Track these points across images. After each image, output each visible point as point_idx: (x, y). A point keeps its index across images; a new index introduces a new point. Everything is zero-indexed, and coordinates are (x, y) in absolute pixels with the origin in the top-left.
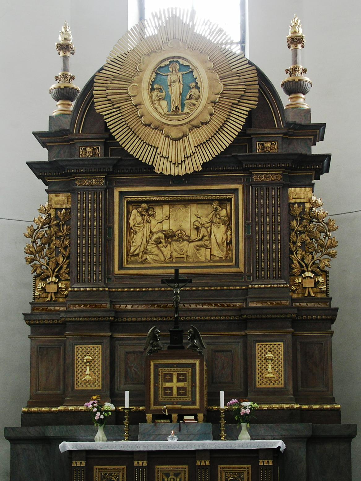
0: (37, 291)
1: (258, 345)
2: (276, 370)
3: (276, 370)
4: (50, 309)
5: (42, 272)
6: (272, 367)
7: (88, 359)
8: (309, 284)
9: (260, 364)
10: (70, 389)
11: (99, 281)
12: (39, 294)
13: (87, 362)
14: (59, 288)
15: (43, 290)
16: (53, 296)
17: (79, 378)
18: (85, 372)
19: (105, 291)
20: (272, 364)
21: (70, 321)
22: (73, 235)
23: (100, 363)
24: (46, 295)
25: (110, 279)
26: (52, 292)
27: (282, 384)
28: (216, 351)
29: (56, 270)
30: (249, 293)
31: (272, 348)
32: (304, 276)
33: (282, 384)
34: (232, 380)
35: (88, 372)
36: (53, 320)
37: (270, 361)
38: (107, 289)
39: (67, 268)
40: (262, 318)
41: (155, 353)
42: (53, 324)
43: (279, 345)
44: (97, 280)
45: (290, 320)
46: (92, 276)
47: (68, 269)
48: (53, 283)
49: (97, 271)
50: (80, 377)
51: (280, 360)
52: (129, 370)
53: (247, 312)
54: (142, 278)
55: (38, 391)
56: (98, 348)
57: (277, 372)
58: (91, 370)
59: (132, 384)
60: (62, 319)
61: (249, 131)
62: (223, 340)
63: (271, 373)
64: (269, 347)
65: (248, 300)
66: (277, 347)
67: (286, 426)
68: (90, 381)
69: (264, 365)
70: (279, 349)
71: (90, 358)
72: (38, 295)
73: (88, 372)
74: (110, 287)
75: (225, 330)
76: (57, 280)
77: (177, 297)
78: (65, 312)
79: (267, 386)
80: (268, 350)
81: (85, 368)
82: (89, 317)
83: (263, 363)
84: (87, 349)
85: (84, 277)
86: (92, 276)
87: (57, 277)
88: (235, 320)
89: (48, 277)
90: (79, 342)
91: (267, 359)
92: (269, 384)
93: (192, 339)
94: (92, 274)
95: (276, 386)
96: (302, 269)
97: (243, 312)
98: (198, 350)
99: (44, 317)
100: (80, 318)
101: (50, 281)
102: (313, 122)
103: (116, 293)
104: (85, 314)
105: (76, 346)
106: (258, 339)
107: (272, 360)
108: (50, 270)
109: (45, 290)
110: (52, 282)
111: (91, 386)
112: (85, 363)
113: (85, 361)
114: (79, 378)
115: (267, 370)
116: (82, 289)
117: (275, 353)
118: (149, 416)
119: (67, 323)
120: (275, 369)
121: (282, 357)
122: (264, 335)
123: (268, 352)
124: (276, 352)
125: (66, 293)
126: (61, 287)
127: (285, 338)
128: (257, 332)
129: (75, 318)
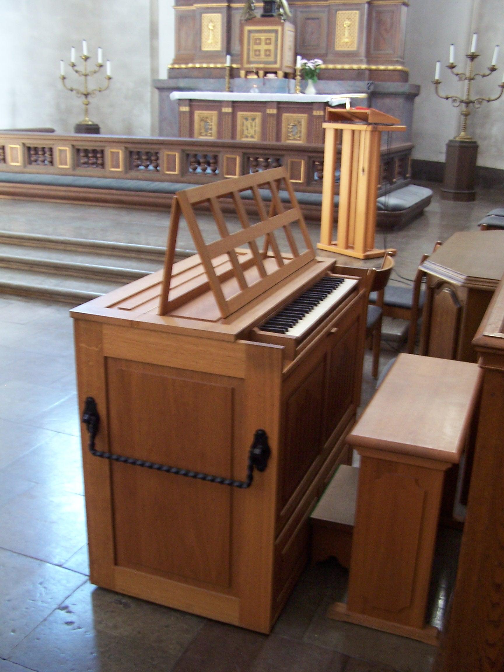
118: (243, 73)
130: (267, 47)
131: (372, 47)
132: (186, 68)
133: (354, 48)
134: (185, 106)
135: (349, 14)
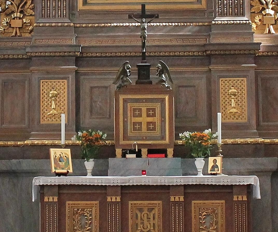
0: (2, 27)
1: (222, 80)
2: (240, 106)
3: (240, 106)
4: (15, 44)
5: (7, 7)
6: (235, 102)
7: (53, 94)
9: (224, 99)
10: (36, 123)
11: (64, 16)
12: (4, 29)
13: (53, 97)
14: (23, 24)
15: (8, 25)
16: (18, 32)
17: (44, 112)
18: (50, 106)
19: (70, 26)
20: (235, 99)
21: (35, 56)
23: (66, 98)
24: (11, 30)
25: (74, 14)
26: (16, 27)
27: (245, 119)
28: (180, 87)
29: (20, 6)
30: (212, 30)
31: (235, 83)
32: (264, 14)
33: (245, 119)
34: (196, 115)
35: (53, 106)
36: (18, 55)
37: (233, 97)
38: (72, 24)
39: (32, 3)
40: (226, 54)
41: (122, 89)
42: (18, 59)
43: (242, 80)
44: (62, 16)
45: (252, 56)
46: (57, 11)
47: (33, 5)
48: (18, 18)
49: (62, 6)
50: (45, 111)
51: (244, 95)
52: (93, 104)
53: (212, 48)
54: (105, 14)
55: (3, 125)
56: (64, 83)
57: (241, 107)
58: (57, 104)
59: (97, 118)
60: (28, 54)
62: (186, 76)
63: (235, 108)
64: (232, 82)
65: (211, 37)
66: (240, 82)
67: (252, 160)
68: (55, 115)
69: (227, 100)
70: (242, 84)
71: (55, 92)
72: (3, 30)
73: (53, 106)
74: (74, 23)
75: (191, 65)
76: (22, 15)
77: (145, 32)
78: (32, 47)
79: (231, 120)
80: (231, 85)
81: (50, 102)
82: (55, 52)
83: (226, 99)
84: (53, 84)
85: (48, 13)
86: (57, 11)
87: (21, 12)
88: (199, 56)
89: (13, 12)
90: (46, 76)
91: (230, 95)
92: (233, 119)
93: (160, 75)
94: (57, 9)
95: (239, 121)
96: (263, 6)
97: (207, 48)
98: (166, 86)
99: (9, 52)
100: (46, 53)
101: (15, 16)
103: (81, 29)
104: (50, 49)
105: (42, 81)
106: (222, 74)
107: (235, 95)
108: (15, 6)
109: (10, 25)
110: (17, 17)
111: (57, 120)
112: (51, 98)
113: (50, 95)
114: (44, 112)
115: (231, 105)
116: (47, 24)
117: (238, 88)
119: (33, 58)
120: (239, 105)
121: (245, 92)
122: (228, 71)
123: (232, 88)
124: (239, 87)
125: (31, 28)
126: (25, 22)
127: (248, 74)
128: (221, 67)
129: (41, 53)
130: (150, 119)
131: (261, 119)
132: (14, 146)
133: (243, 120)
134: (53, 195)
135: (235, 81)
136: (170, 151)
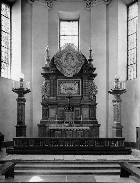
8: (92, 98)
22: (50, 88)
61: (82, 69)
102: (94, 67)
136: (74, 122)
